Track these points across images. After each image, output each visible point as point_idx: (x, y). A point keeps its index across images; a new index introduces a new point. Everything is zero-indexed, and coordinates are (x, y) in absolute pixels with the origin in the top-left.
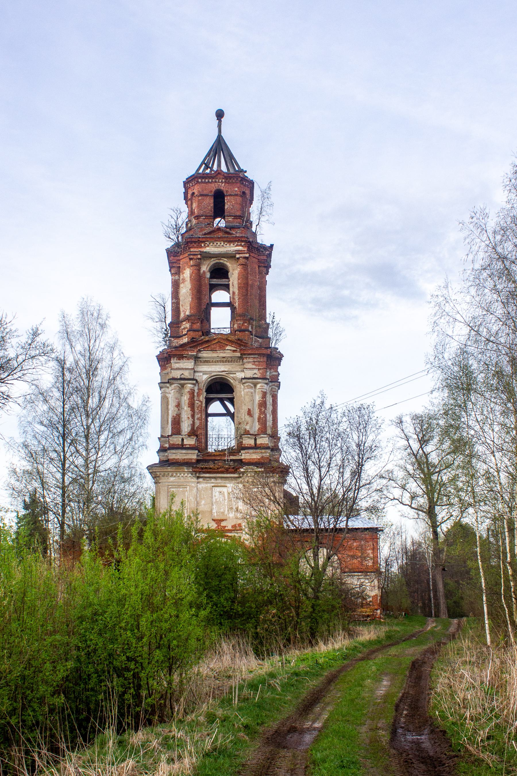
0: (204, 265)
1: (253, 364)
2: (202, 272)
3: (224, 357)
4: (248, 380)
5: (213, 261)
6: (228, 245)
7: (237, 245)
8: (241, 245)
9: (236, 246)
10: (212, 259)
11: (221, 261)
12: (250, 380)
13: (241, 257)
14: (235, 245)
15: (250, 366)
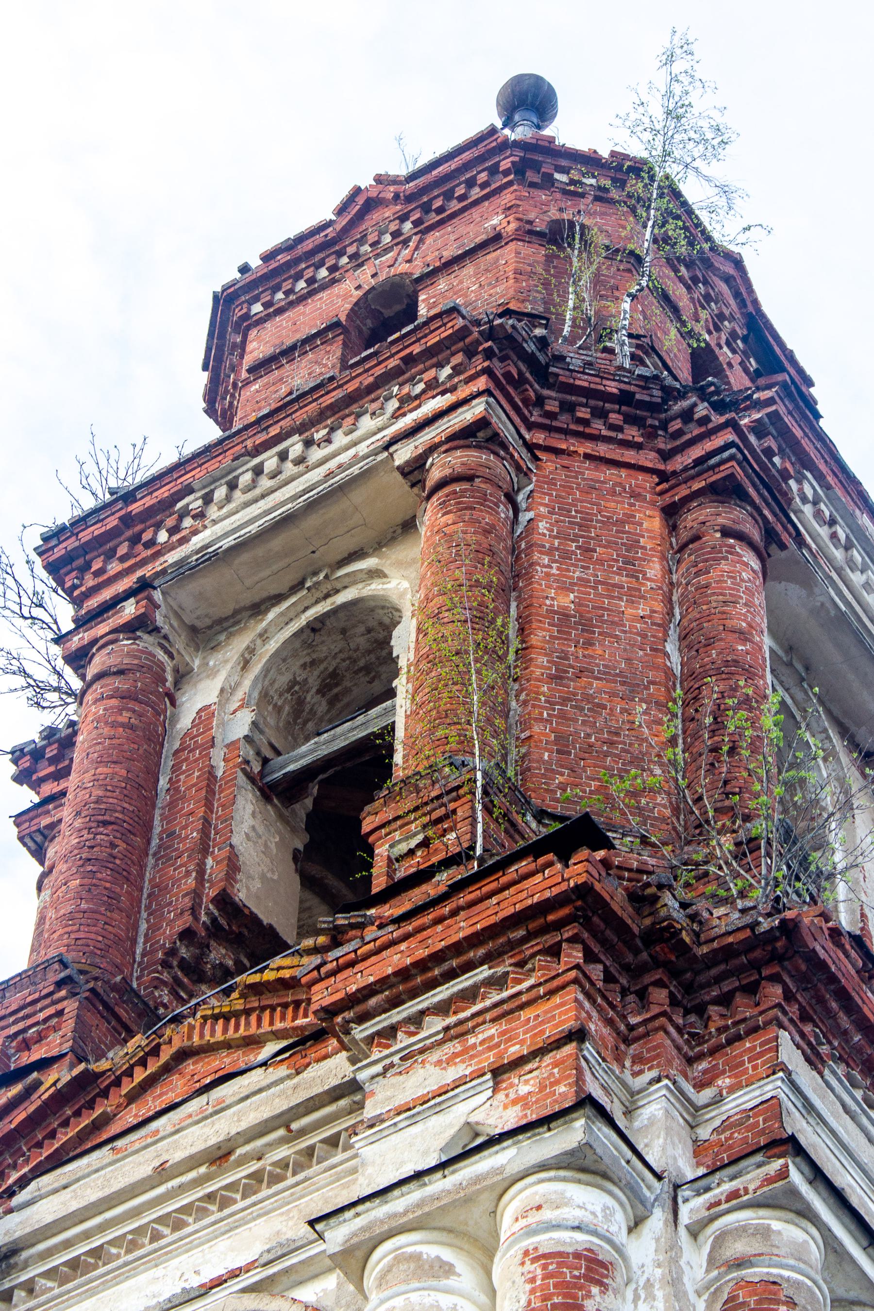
0: (213, 674)
1: (450, 1061)
2: (185, 722)
3: (220, 1156)
4: (379, 1211)
5: (278, 628)
6: (340, 439)
7: (408, 402)
8: (433, 387)
9: (397, 415)
10: (271, 615)
11: (341, 598)
12: (398, 1203)
13: (432, 449)
14: (393, 404)
15: (426, 1077)
